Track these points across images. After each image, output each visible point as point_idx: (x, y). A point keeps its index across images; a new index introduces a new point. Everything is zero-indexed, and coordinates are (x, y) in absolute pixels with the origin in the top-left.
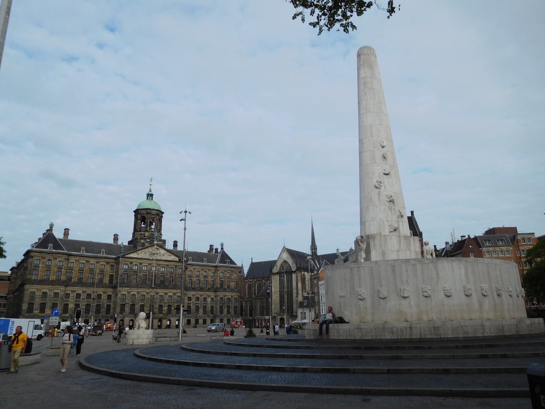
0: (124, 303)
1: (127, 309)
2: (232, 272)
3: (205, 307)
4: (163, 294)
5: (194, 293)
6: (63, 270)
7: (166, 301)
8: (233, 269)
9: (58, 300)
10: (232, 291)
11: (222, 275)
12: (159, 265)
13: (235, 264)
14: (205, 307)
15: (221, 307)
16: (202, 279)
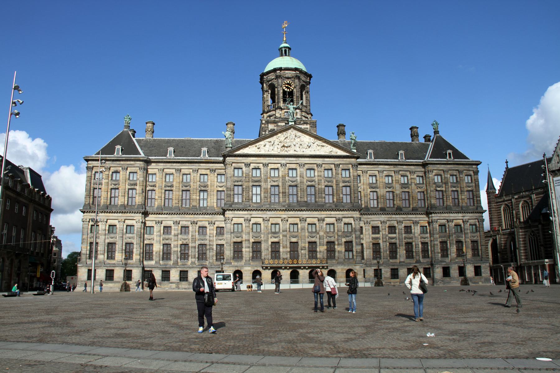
0: (239, 240)
1: (247, 251)
2: (460, 172)
3: (409, 245)
4: (315, 221)
5: (383, 218)
6: (137, 187)
7: (322, 233)
8: (461, 167)
9: (133, 238)
10: (463, 210)
11: (437, 179)
12: (302, 165)
13: (465, 158)
14: (409, 245)
15: (443, 243)
16: (398, 190)
